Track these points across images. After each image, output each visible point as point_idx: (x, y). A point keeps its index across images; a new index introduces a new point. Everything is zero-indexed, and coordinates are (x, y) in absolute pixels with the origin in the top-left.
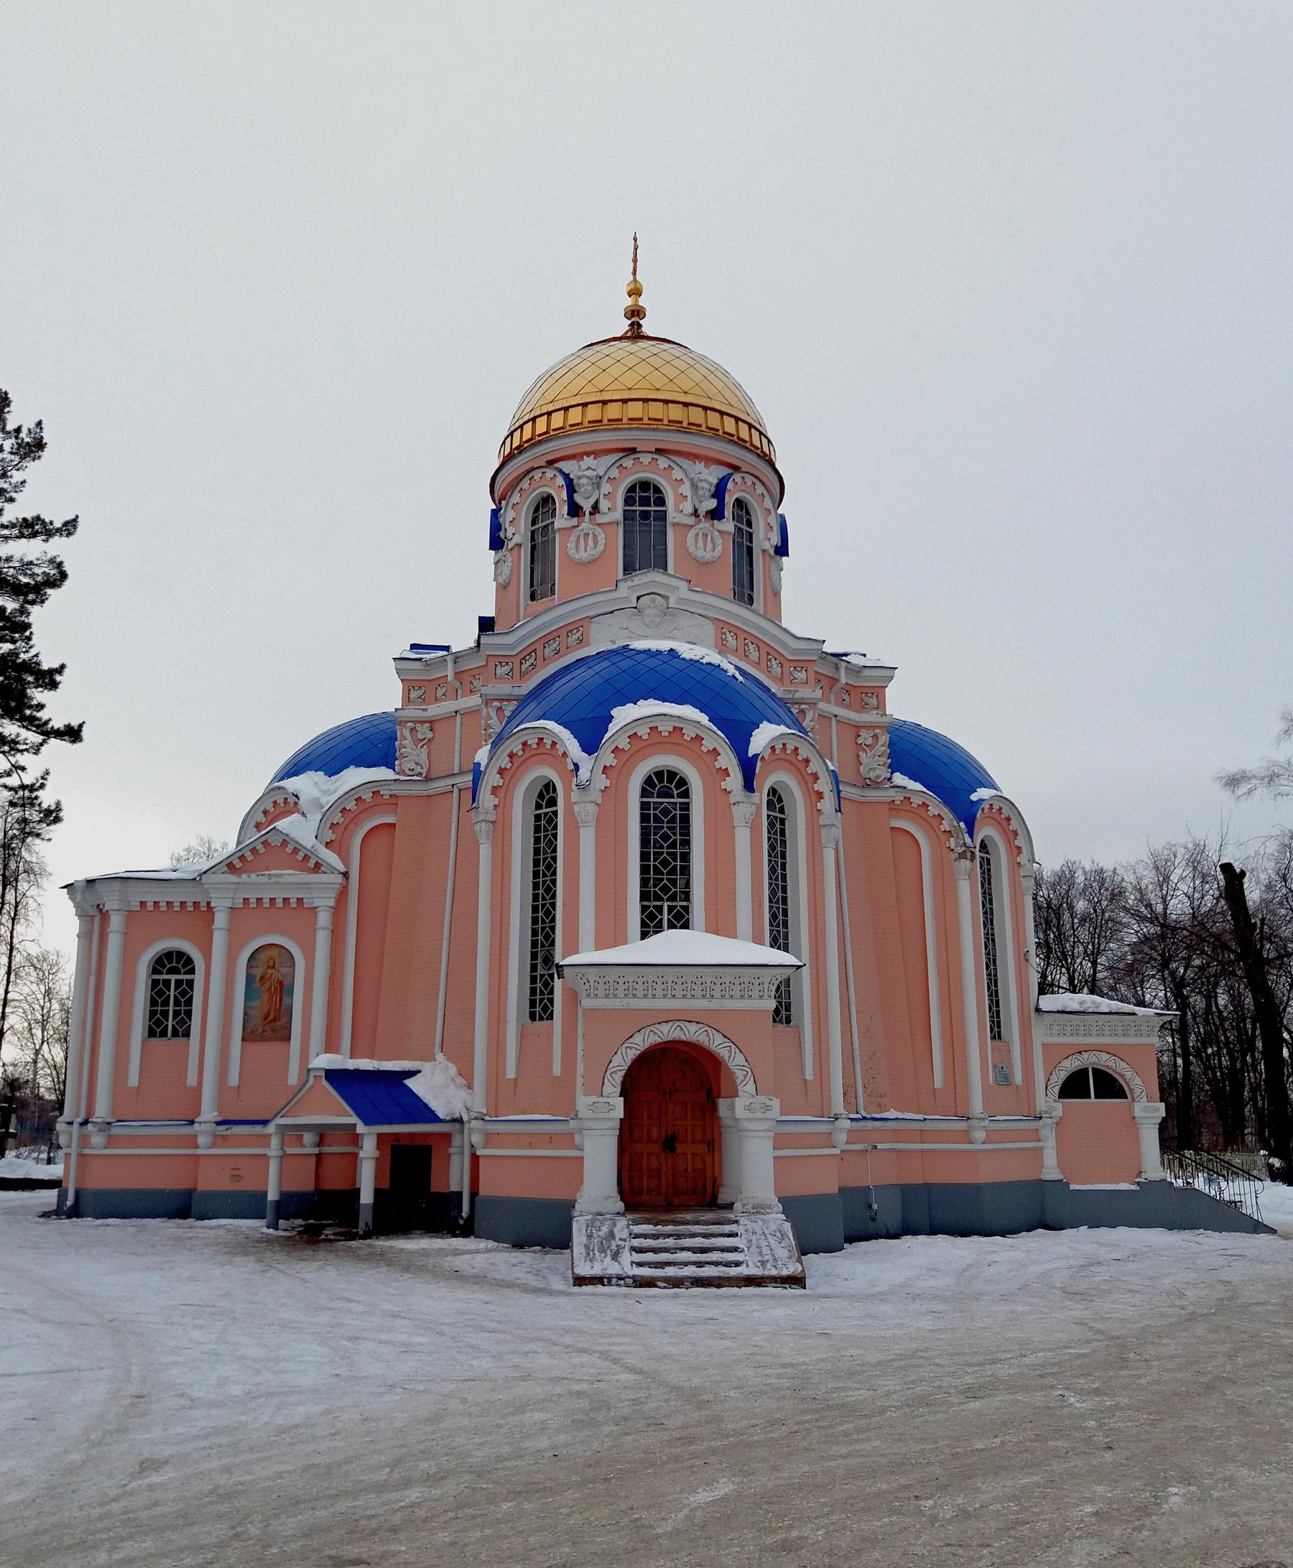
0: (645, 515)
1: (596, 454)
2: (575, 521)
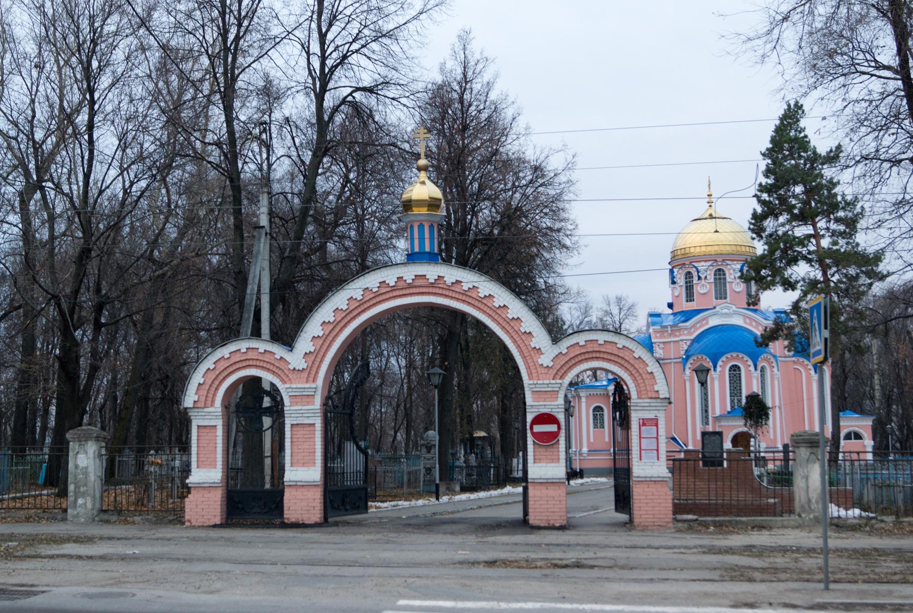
1: (705, 261)
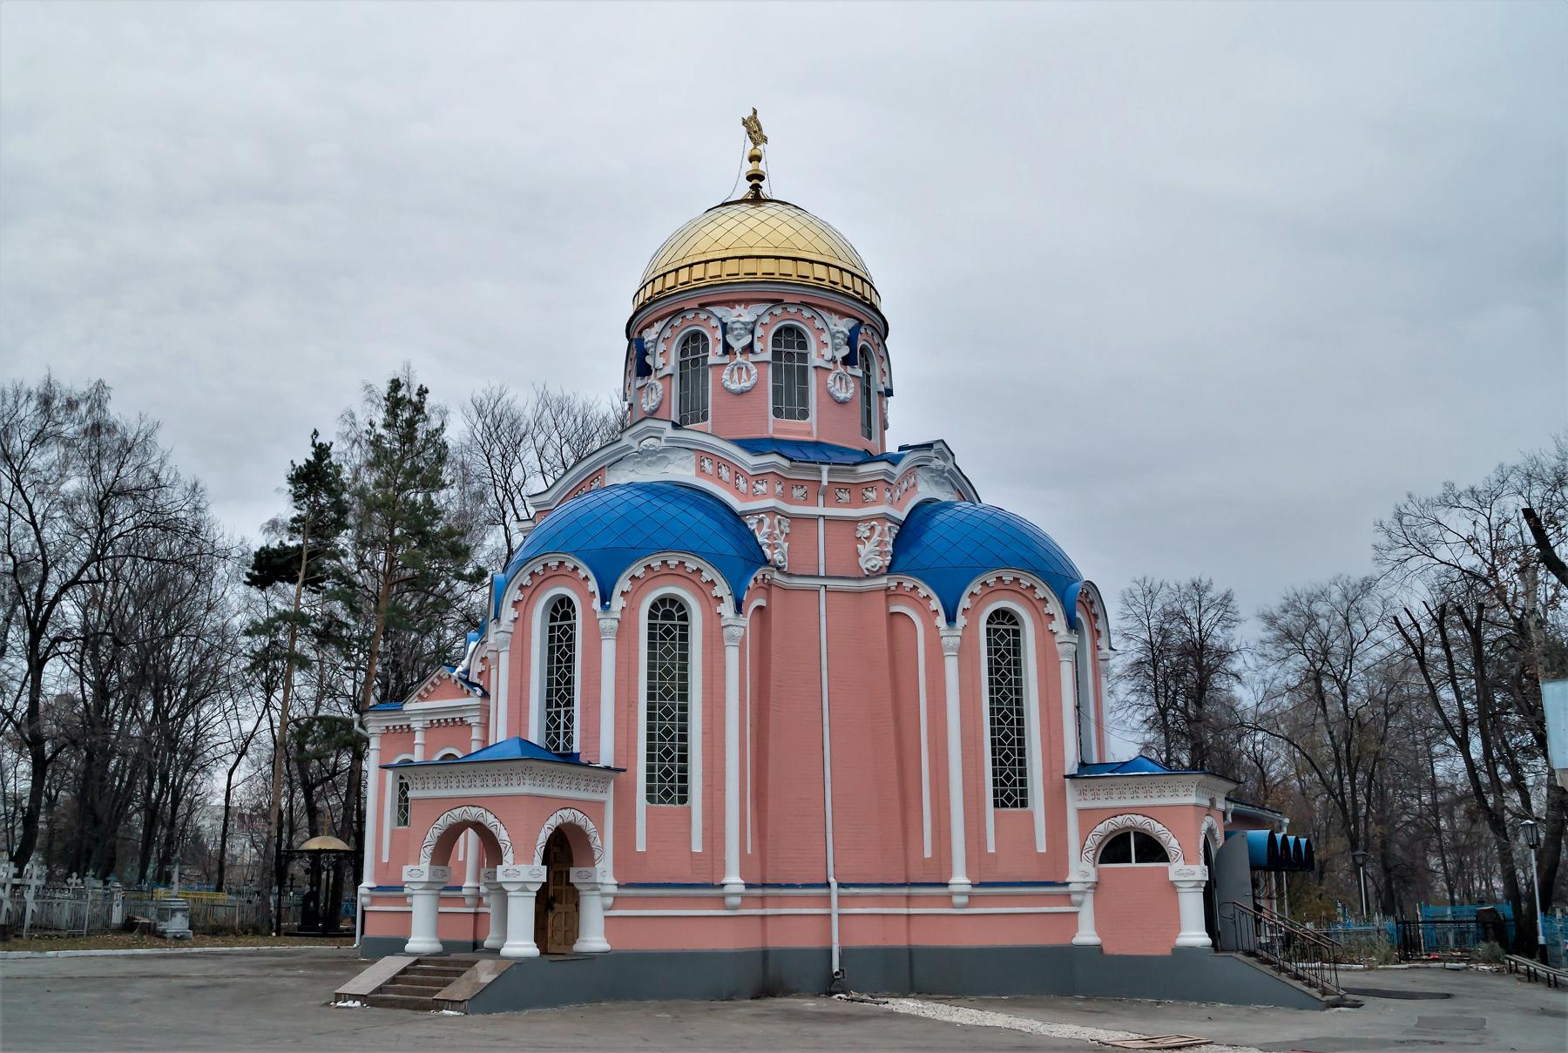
0: (790, 356)
1: (747, 302)
2: (726, 359)
